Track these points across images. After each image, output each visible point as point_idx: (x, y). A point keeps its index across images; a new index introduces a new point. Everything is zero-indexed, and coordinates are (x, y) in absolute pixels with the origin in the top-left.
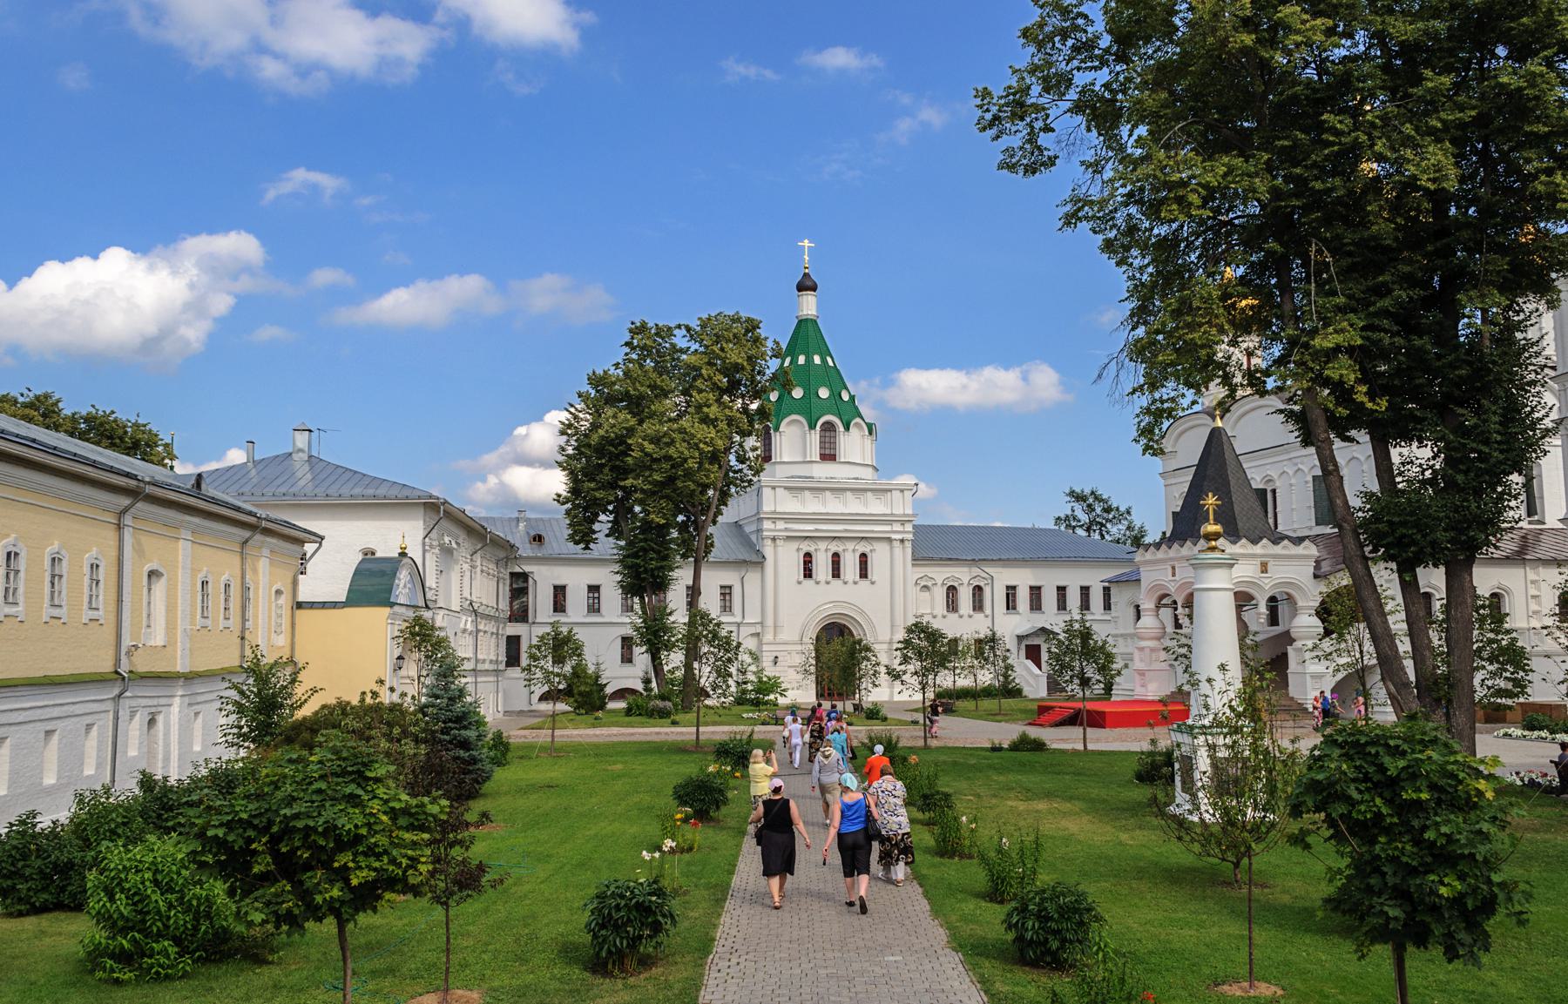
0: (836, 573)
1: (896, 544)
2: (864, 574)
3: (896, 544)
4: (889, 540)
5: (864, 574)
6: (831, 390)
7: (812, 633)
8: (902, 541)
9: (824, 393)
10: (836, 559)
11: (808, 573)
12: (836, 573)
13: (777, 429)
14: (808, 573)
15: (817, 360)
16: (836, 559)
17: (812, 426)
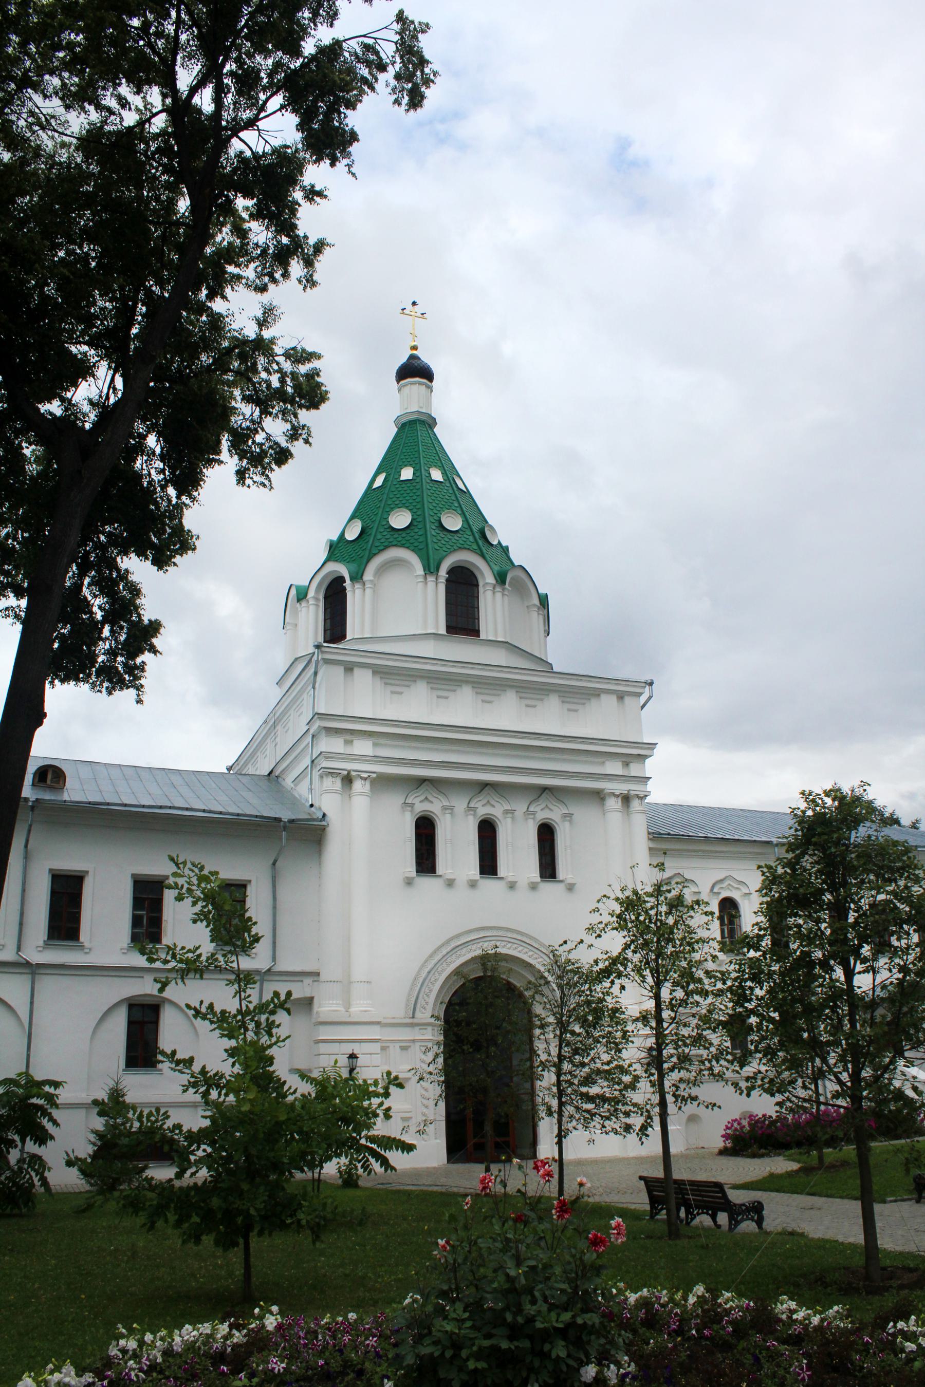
0: (488, 864)
1: (613, 804)
2: (548, 868)
3: (613, 804)
4: (599, 796)
5: (548, 868)
6: (466, 520)
7: (430, 1008)
8: (626, 799)
9: (453, 523)
10: (487, 832)
11: (426, 861)
12: (488, 864)
13: (357, 577)
14: (426, 861)
15: (437, 475)
16: (487, 832)
17: (431, 569)
